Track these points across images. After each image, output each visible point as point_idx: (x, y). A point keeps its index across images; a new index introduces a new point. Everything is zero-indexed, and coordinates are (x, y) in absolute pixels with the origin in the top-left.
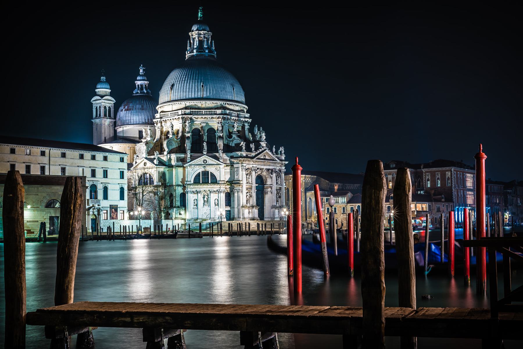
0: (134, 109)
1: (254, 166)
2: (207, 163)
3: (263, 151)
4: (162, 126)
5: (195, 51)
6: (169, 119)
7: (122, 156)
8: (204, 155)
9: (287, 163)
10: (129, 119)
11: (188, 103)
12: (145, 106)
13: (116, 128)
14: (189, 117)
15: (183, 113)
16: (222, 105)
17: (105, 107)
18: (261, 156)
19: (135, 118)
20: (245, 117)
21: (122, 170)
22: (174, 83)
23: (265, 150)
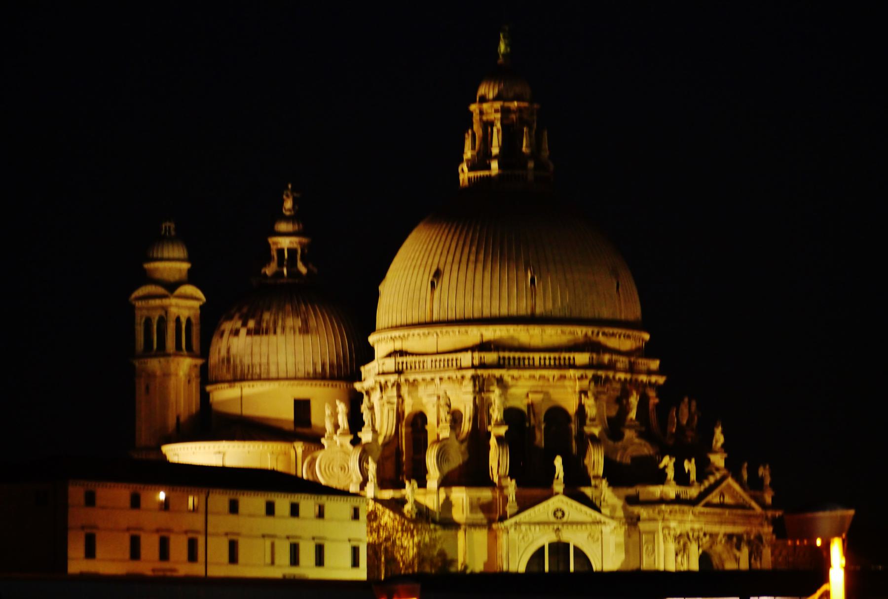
0: (279, 330)
1: (697, 526)
2: (565, 519)
3: (718, 483)
4: (399, 396)
5: (495, 165)
6: (428, 377)
7: (355, 502)
8: (557, 494)
9: (778, 514)
10: (264, 360)
11: (491, 333)
12: (312, 323)
13: (208, 388)
14: (494, 377)
15: (476, 362)
16: (590, 338)
17: (178, 320)
18: (714, 498)
19: (282, 359)
20: (650, 373)
21: (355, 544)
22: (441, 267)
23: (723, 478)
